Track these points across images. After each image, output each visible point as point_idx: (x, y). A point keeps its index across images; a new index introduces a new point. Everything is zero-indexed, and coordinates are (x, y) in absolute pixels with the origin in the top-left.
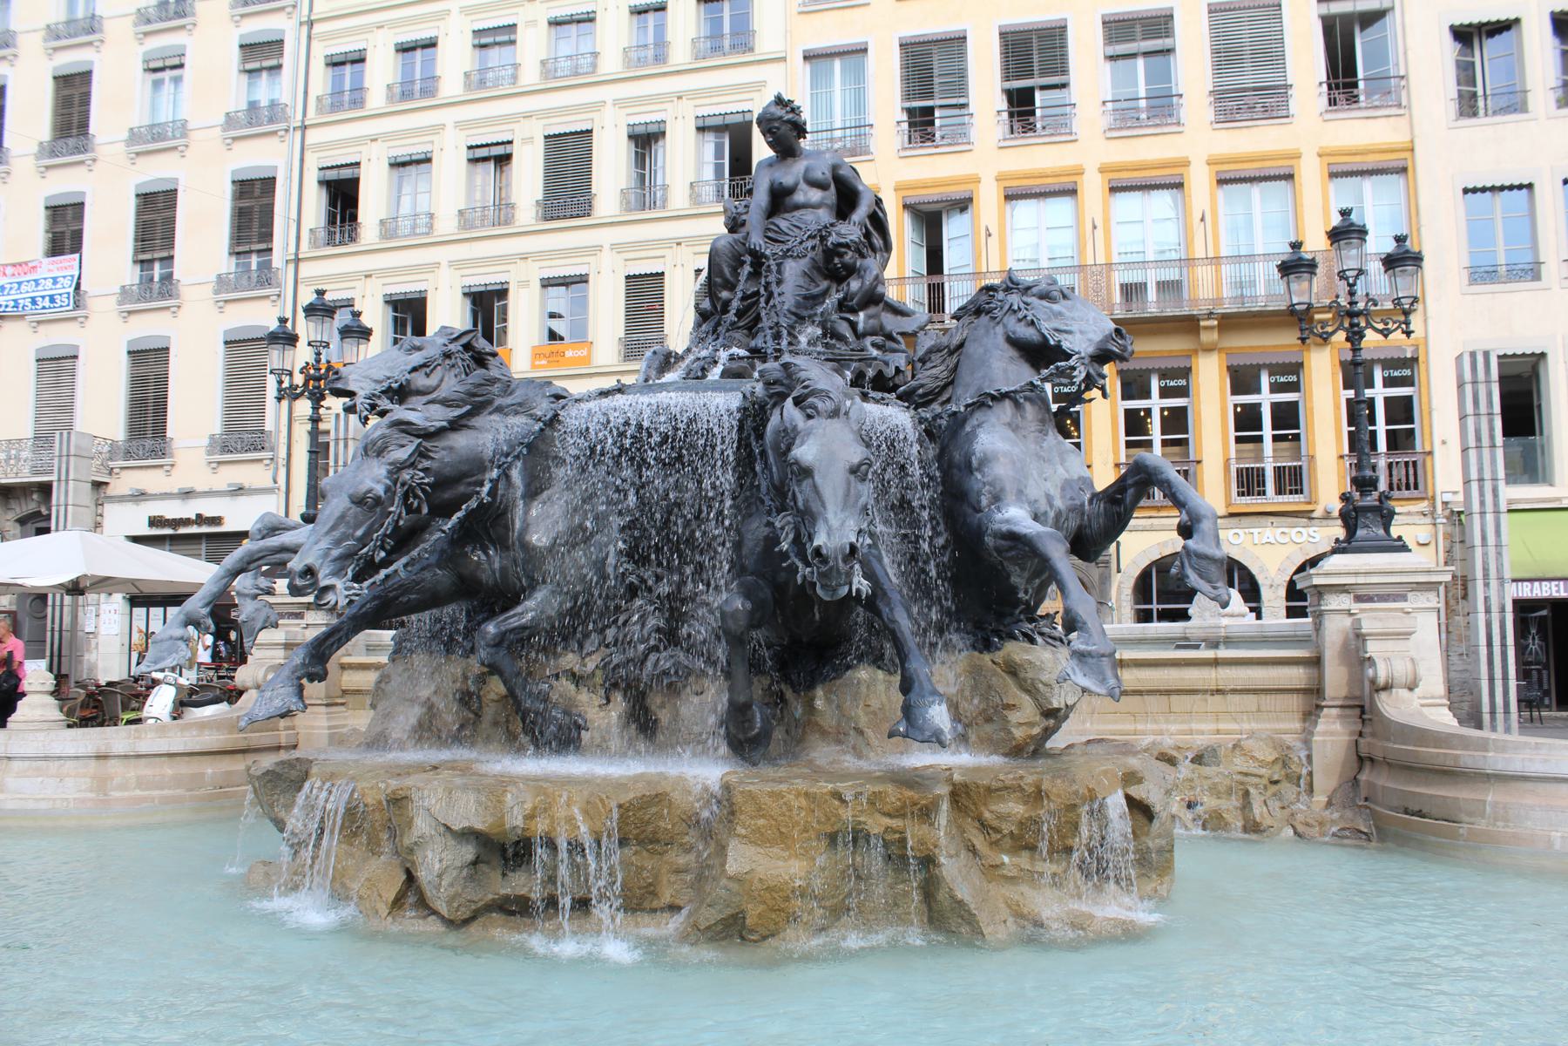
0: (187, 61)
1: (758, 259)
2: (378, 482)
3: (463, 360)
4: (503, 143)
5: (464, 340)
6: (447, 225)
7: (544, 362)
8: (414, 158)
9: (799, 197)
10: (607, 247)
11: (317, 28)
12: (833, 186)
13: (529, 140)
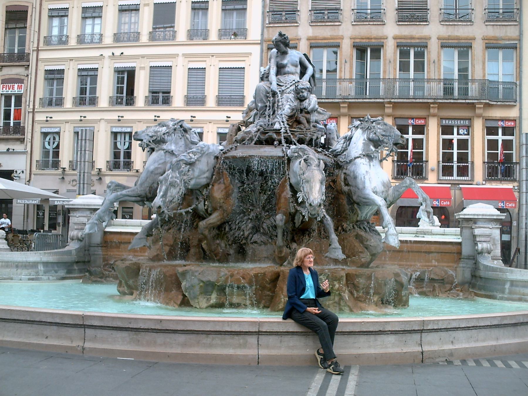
1: (274, 94)
3: (180, 131)
5: (180, 124)
6: (108, 40)
9: (287, 69)
10: (180, 54)
12: (299, 66)
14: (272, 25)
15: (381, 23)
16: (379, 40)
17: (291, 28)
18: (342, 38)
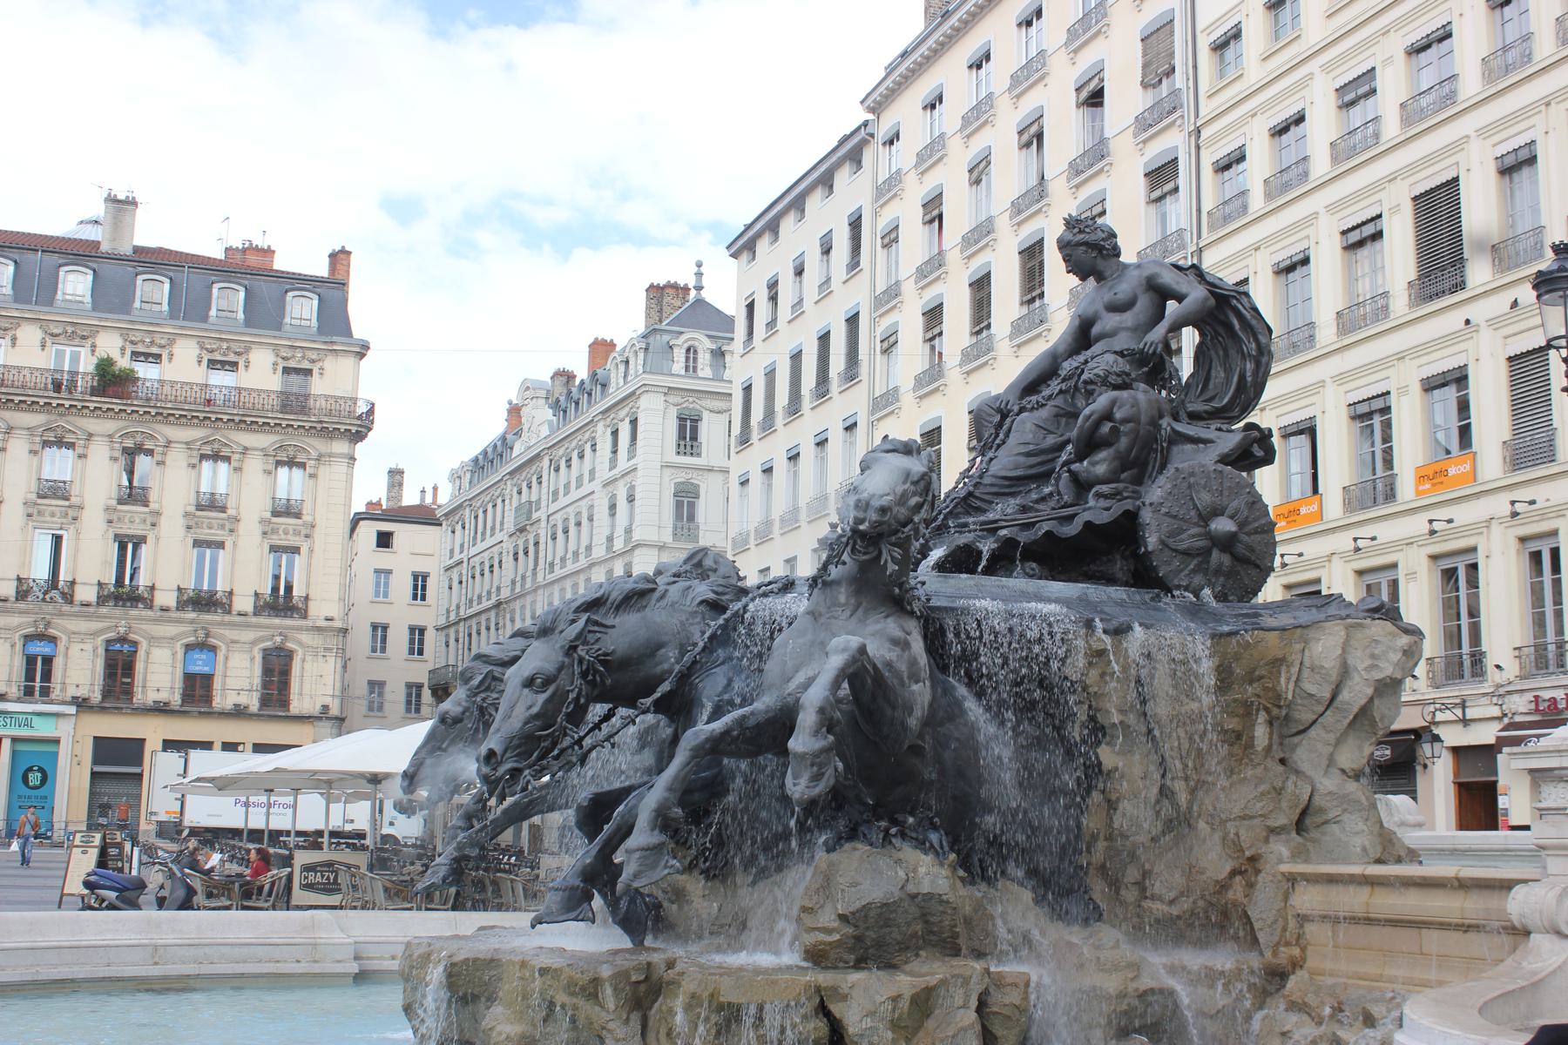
0: (1108, 206)
2: (460, 704)
4: (1373, 219)
5: (695, 561)
7: (1428, 486)
8: (1294, 259)
9: (1096, 330)
11: (1205, 134)
13: (1396, 209)
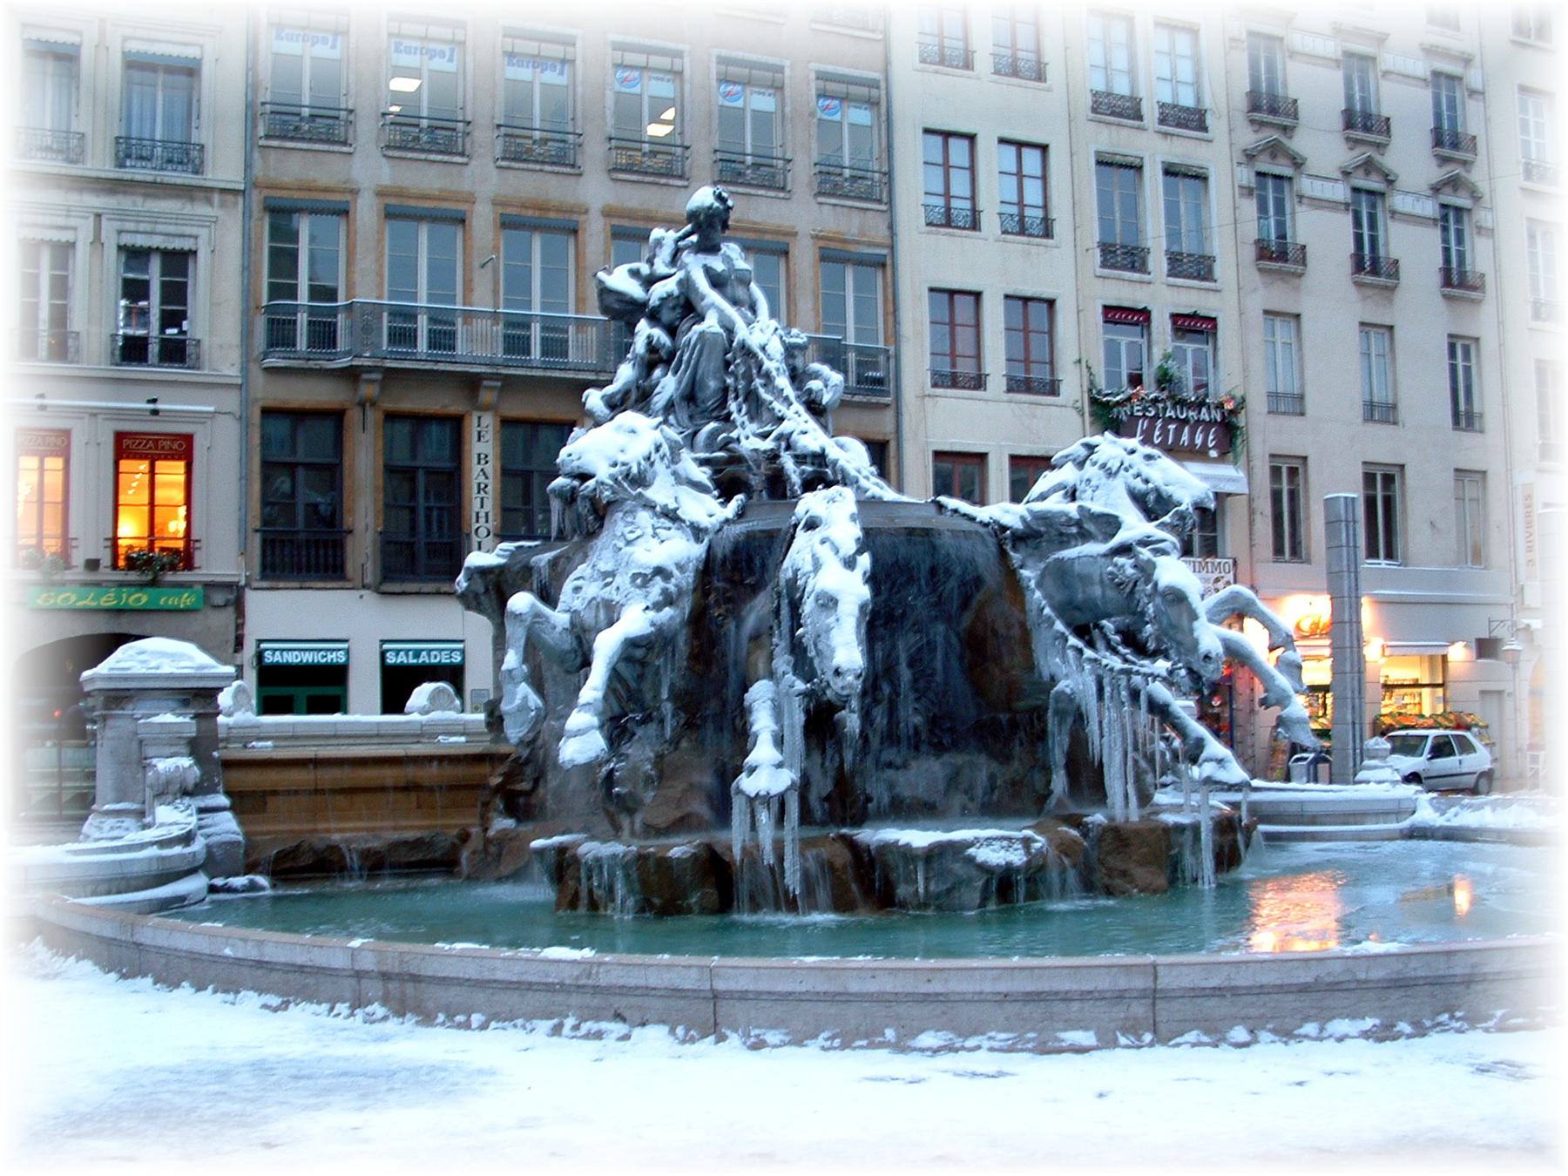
14: (275, 143)
15: (568, 170)
16: (567, 216)
17: (332, 157)
18: (470, 199)
